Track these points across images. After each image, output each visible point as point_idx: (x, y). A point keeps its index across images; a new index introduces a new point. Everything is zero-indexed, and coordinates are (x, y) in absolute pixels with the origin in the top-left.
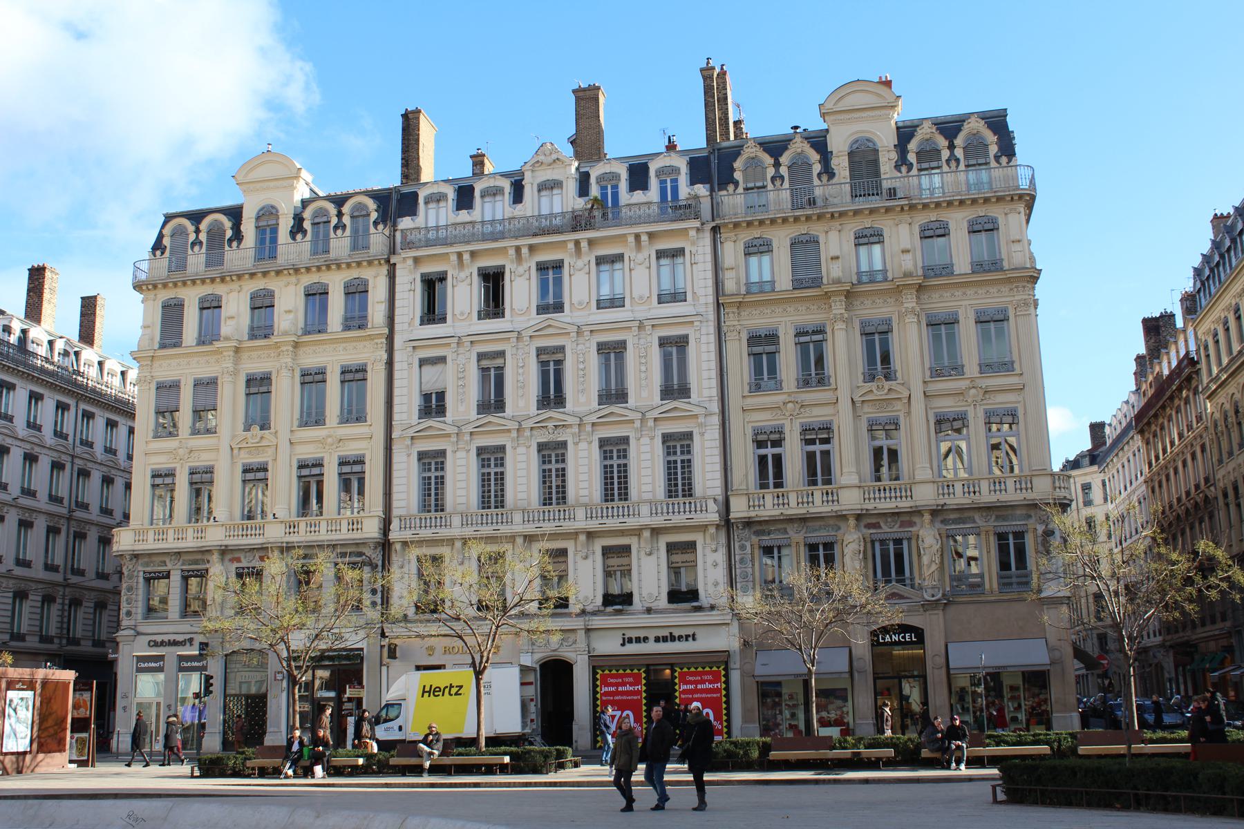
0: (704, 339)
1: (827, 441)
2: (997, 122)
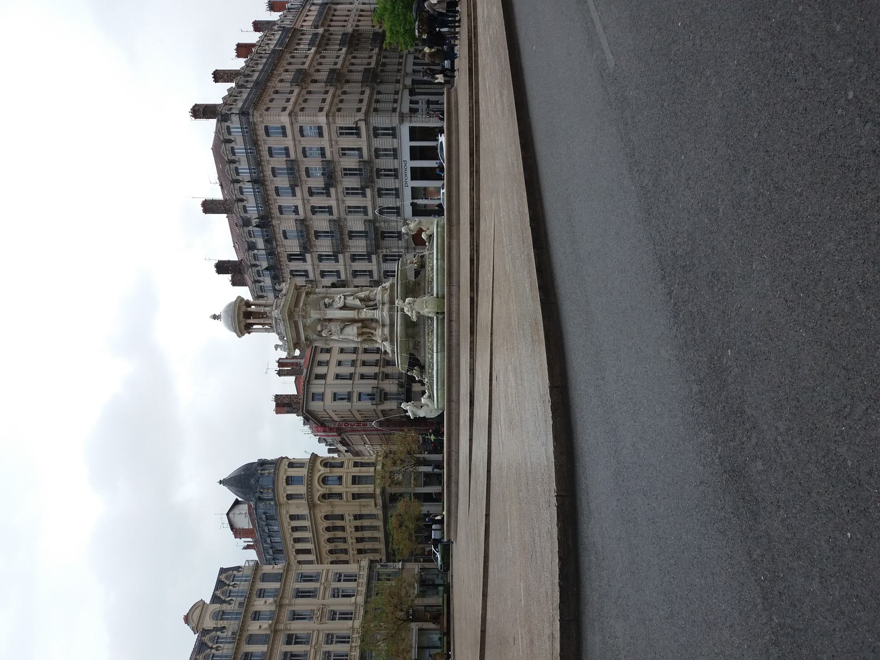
1: (332, 638)
2: (223, 571)
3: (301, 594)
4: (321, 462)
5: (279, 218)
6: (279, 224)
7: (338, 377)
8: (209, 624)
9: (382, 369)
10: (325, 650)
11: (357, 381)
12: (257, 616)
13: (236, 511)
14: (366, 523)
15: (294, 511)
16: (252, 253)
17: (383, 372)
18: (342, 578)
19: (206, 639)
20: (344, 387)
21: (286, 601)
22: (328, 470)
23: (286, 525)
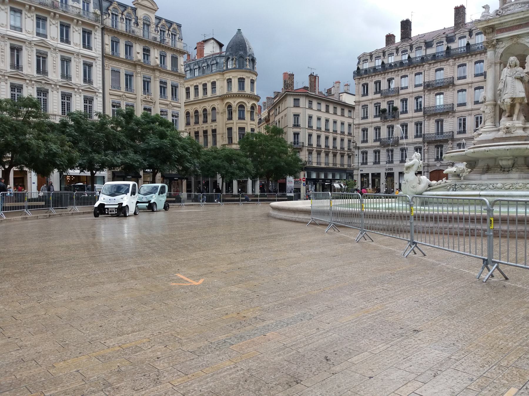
0: (98, 66)
3: (163, 86)
4: (254, 104)
5: (454, 64)
6: (449, 65)
7: (310, 117)
8: (141, 13)
9: (315, 149)
10: (122, 103)
11: (308, 131)
12: (146, 52)
13: (216, 45)
14: (210, 138)
15: (218, 84)
16: (423, 45)
17: (313, 150)
18: (174, 118)
19: (129, 10)
20: (303, 122)
21: (157, 74)
22: (249, 109)
23: (208, 79)
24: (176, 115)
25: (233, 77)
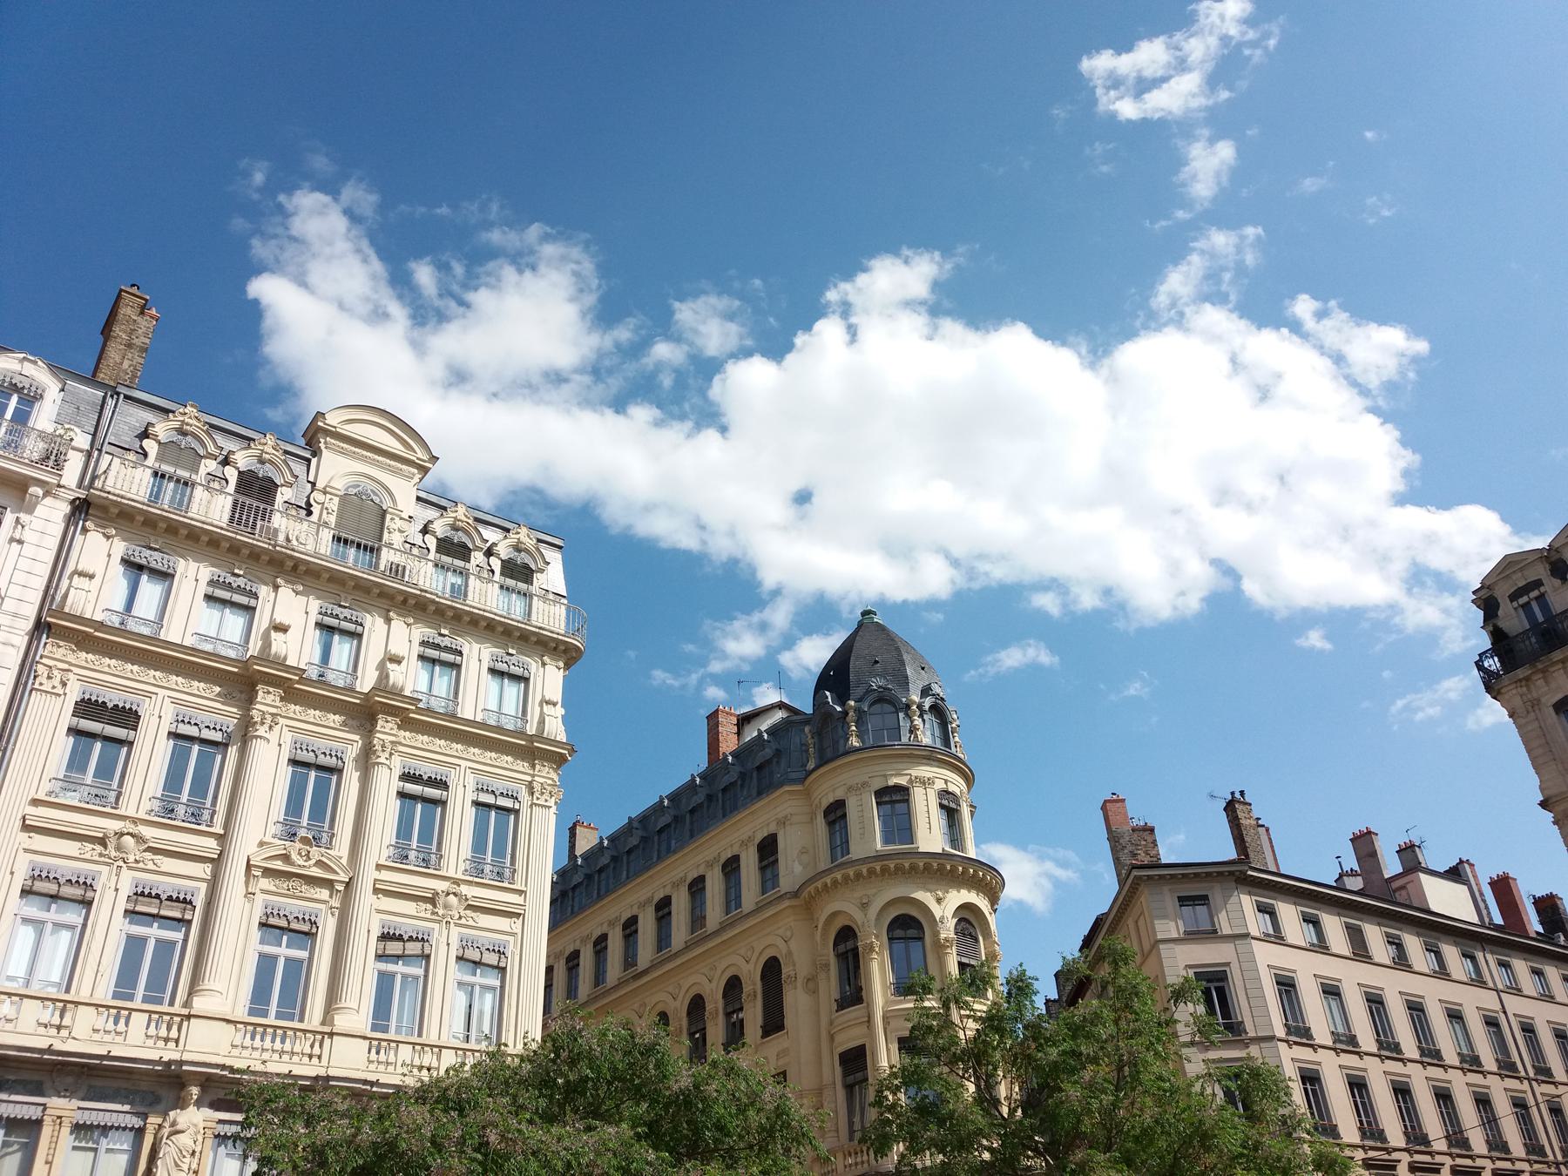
3: (423, 797)
24: (491, 959)
25: (850, 789)
